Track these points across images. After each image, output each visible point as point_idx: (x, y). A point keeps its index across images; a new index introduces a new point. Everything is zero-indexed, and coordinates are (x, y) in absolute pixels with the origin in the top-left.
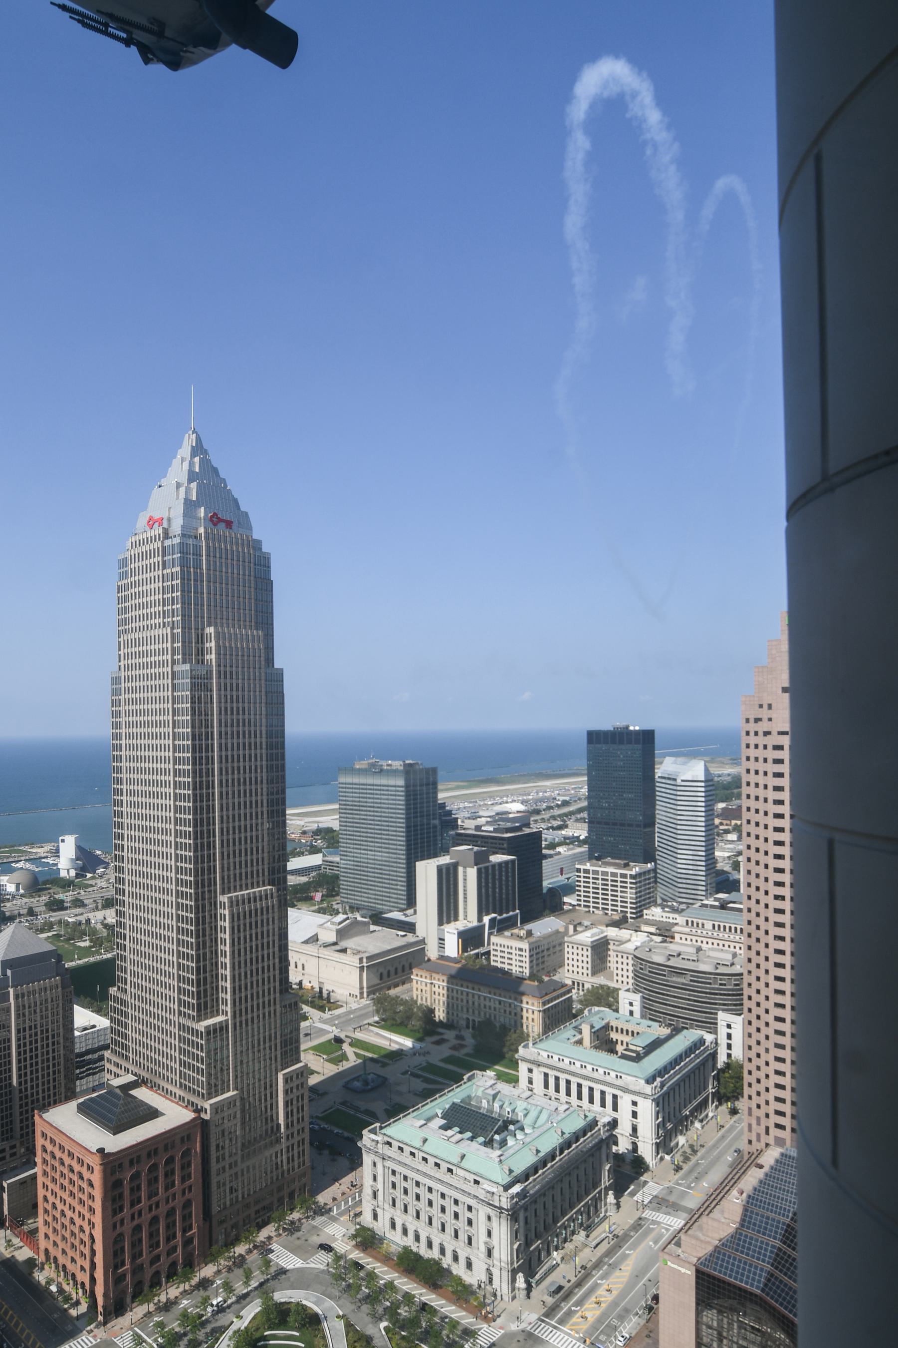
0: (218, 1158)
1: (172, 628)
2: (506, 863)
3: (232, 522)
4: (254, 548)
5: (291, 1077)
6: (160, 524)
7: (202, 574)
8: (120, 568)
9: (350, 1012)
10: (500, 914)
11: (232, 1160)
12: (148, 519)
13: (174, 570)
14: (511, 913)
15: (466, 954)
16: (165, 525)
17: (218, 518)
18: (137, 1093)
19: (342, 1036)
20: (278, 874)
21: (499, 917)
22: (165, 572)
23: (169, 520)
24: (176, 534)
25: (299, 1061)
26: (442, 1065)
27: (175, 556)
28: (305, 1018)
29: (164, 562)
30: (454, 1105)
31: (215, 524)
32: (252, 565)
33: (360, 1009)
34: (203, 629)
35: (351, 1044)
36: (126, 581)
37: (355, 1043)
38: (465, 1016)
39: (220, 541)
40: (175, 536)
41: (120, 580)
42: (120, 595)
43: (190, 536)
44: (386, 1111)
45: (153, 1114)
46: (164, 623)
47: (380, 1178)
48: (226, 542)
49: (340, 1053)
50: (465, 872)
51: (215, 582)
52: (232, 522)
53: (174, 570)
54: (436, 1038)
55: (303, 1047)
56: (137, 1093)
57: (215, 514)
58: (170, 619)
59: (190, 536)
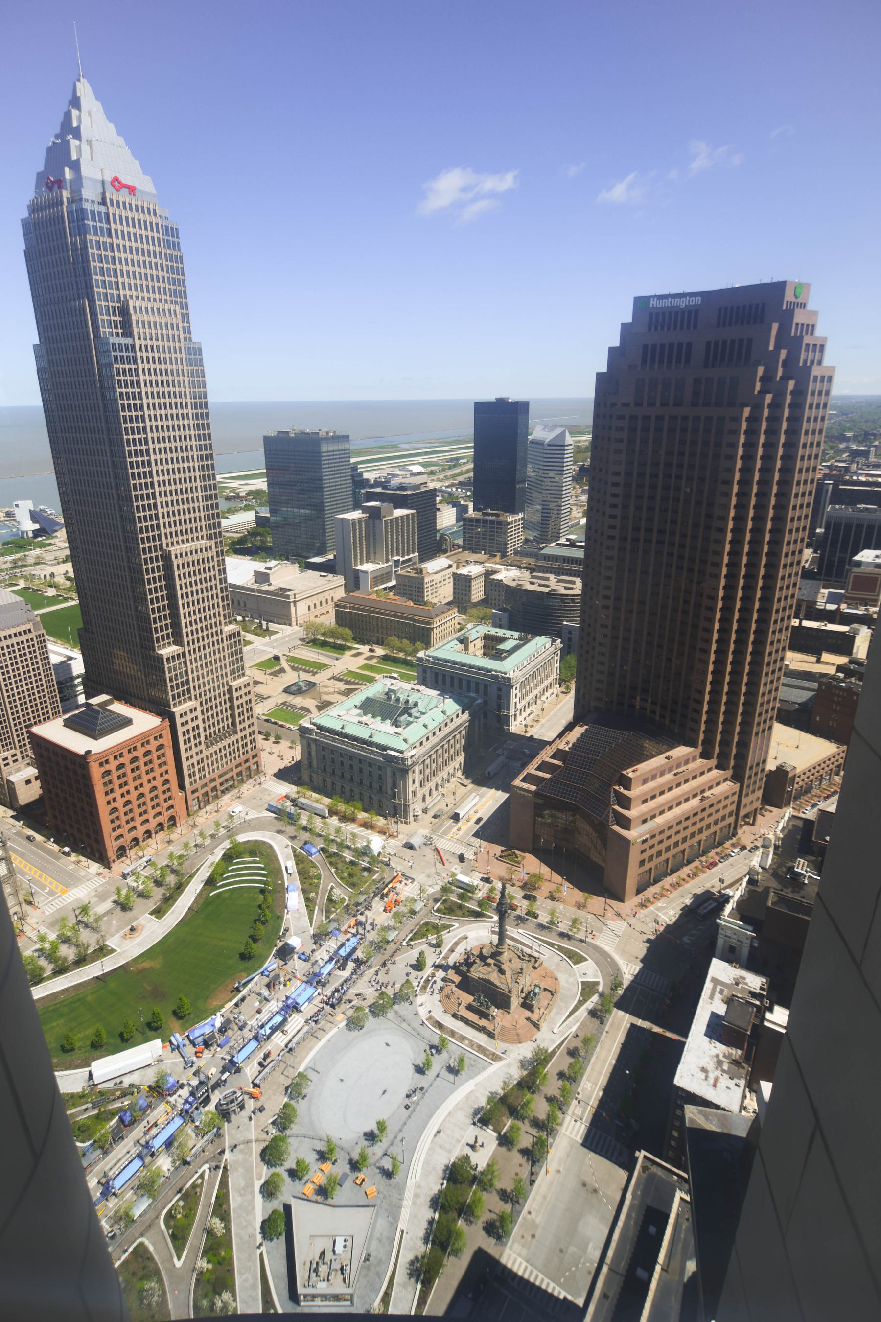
0: (186, 750)
2: (407, 515)
5: (240, 688)
9: (286, 637)
10: (403, 556)
11: (198, 749)
14: (411, 555)
15: (375, 589)
18: (110, 708)
19: (280, 655)
20: (215, 532)
21: (402, 559)
25: (243, 675)
26: (359, 671)
28: (250, 643)
30: (368, 699)
31: (117, 190)
33: (293, 634)
35: (287, 661)
37: (291, 659)
38: (376, 635)
44: (317, 706)
45: (128, 722)
47: (314, 753)
49: (279, 667)
50: (374, 524)
54: (354, 652)
55: (247, 665)
56: (110, 708)
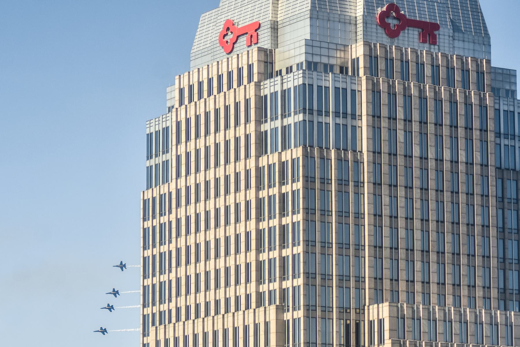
1: (281, 309)
3: (436, 27)
4: (495, 92)
6: (253, 40)
7: (358, 162)
8: (149, 157)
12: (221, 28)
13: (286, 156)
16: (265, 41)
17: (400, 17)
22: (264, 161)
23: (275, 28)
24: (293, 62)
27: (290, 121)
29: (261, 138)
31: (393, 34)
32: (491, 136)
34: (360, 310)
36: (164, 189)
39: (405, 77)
40: (289, 70)
41: (149, 186)
42: (148, 224)
43: (328, 68)
46: (260, 296)
48: (420, 78)
51: (393, 186)
52: (436, 27)
53: (286, 156)
57: (392, 7)
58: (275, 286)
59: (328, 68)
